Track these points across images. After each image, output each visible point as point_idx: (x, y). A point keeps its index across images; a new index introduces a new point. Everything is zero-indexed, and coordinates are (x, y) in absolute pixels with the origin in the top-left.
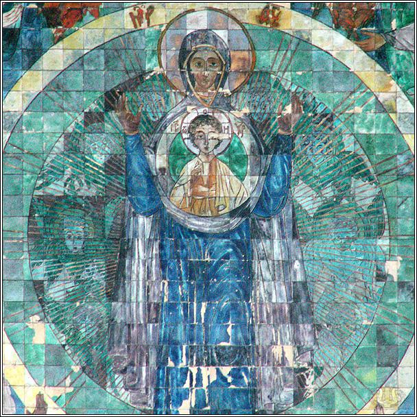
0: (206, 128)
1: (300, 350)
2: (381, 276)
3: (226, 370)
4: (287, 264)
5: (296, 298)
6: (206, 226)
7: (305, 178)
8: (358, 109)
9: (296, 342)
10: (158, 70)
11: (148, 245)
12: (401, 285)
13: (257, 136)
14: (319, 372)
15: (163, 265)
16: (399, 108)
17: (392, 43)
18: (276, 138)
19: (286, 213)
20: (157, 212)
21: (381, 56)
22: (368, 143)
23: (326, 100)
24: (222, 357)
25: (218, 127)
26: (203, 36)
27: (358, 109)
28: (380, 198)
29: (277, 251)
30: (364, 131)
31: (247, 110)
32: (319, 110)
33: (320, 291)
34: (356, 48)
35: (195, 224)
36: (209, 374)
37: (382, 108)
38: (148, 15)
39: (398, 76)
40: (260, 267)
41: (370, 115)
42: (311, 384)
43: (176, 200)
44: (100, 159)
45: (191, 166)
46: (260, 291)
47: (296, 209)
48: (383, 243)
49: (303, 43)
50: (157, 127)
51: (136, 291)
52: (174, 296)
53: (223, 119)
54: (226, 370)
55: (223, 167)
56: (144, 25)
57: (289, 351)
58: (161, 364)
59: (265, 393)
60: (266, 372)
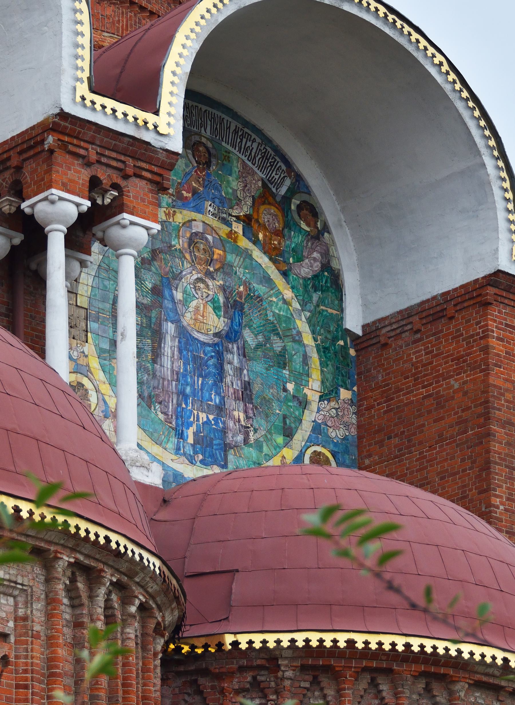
0: (202, 286)
1: (248, 418)
2: (285, 390)
3: (211, 417)
4: (241, 370)
5: (246, 389)
6: (202, 338)
7: (250, 327)
8: (274, 299)
9: (246, 412)
10: (178, 247)
11: (173, 338)
12: (294, 397)
13: (227, 298)
14: (256, 431)
15: (180, 351)
16: (293, 305)
17: (290, 269)
18: (235, 301)
19: (240, 343)
20: (177, 322)
21: (285, 274)
22: (278, 317)
23: (261, 289)
24: (209, 410)
25: (207, 286)
26: (201, 235)
27: (274, 299)
28: (284, 349)
29: (236, 361)
30: (277, 312)
31: (221, 282)
32: (256, 294)
33: (256, 388)
34: (274, 267)
35: (196, 335)
36: (203, 416)
37: (285, 302)
38: (174, 215)
39: (293, 288)
40: (228, 367)
41: (280, 303)
42: (252, 437)
43: (187, 319)
44: (150, 286)
45: (194, 303)
46: (228, 379)
47: (245, 342)
48: (286, 372)
49: (247, 255)
50: (178, 277)
51: (167, 362)
52: (186, 370)
53: (210, 283)
54: (211, 417)
55: (210, 309)
56: (171, 220)
57: (242, 416)
58: (179, 405)
59: (230, 435)
60: (231, 424)
